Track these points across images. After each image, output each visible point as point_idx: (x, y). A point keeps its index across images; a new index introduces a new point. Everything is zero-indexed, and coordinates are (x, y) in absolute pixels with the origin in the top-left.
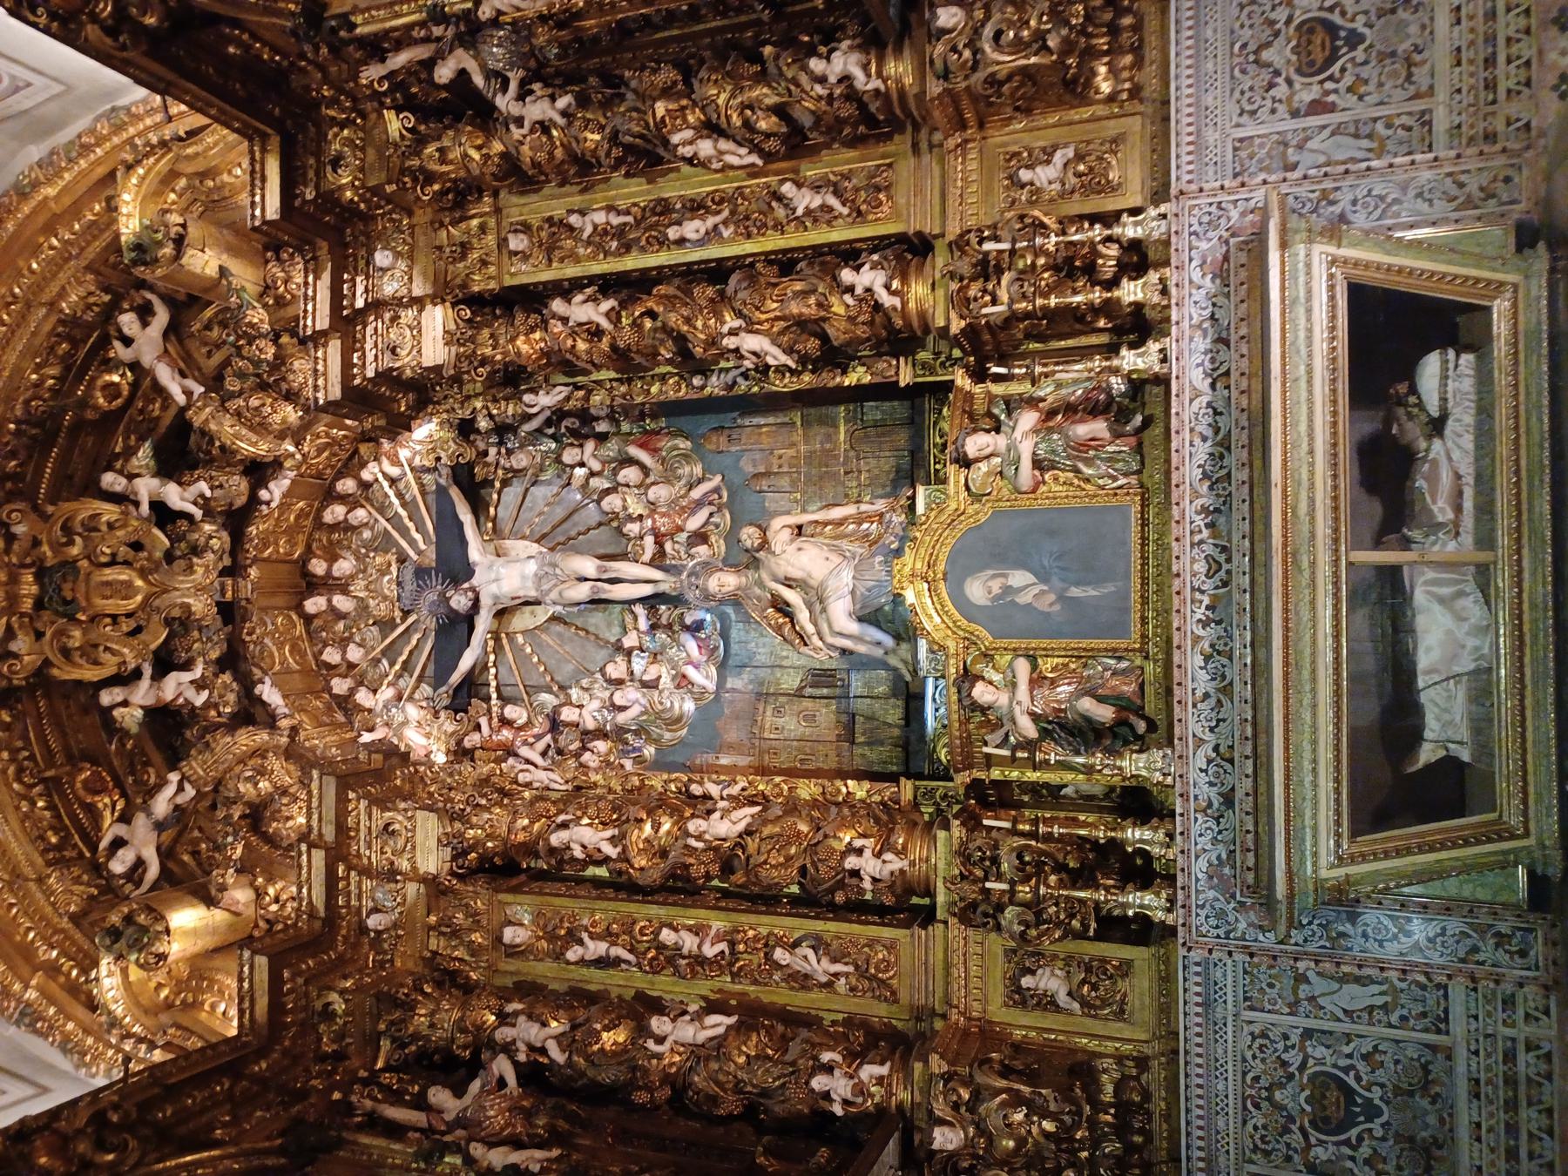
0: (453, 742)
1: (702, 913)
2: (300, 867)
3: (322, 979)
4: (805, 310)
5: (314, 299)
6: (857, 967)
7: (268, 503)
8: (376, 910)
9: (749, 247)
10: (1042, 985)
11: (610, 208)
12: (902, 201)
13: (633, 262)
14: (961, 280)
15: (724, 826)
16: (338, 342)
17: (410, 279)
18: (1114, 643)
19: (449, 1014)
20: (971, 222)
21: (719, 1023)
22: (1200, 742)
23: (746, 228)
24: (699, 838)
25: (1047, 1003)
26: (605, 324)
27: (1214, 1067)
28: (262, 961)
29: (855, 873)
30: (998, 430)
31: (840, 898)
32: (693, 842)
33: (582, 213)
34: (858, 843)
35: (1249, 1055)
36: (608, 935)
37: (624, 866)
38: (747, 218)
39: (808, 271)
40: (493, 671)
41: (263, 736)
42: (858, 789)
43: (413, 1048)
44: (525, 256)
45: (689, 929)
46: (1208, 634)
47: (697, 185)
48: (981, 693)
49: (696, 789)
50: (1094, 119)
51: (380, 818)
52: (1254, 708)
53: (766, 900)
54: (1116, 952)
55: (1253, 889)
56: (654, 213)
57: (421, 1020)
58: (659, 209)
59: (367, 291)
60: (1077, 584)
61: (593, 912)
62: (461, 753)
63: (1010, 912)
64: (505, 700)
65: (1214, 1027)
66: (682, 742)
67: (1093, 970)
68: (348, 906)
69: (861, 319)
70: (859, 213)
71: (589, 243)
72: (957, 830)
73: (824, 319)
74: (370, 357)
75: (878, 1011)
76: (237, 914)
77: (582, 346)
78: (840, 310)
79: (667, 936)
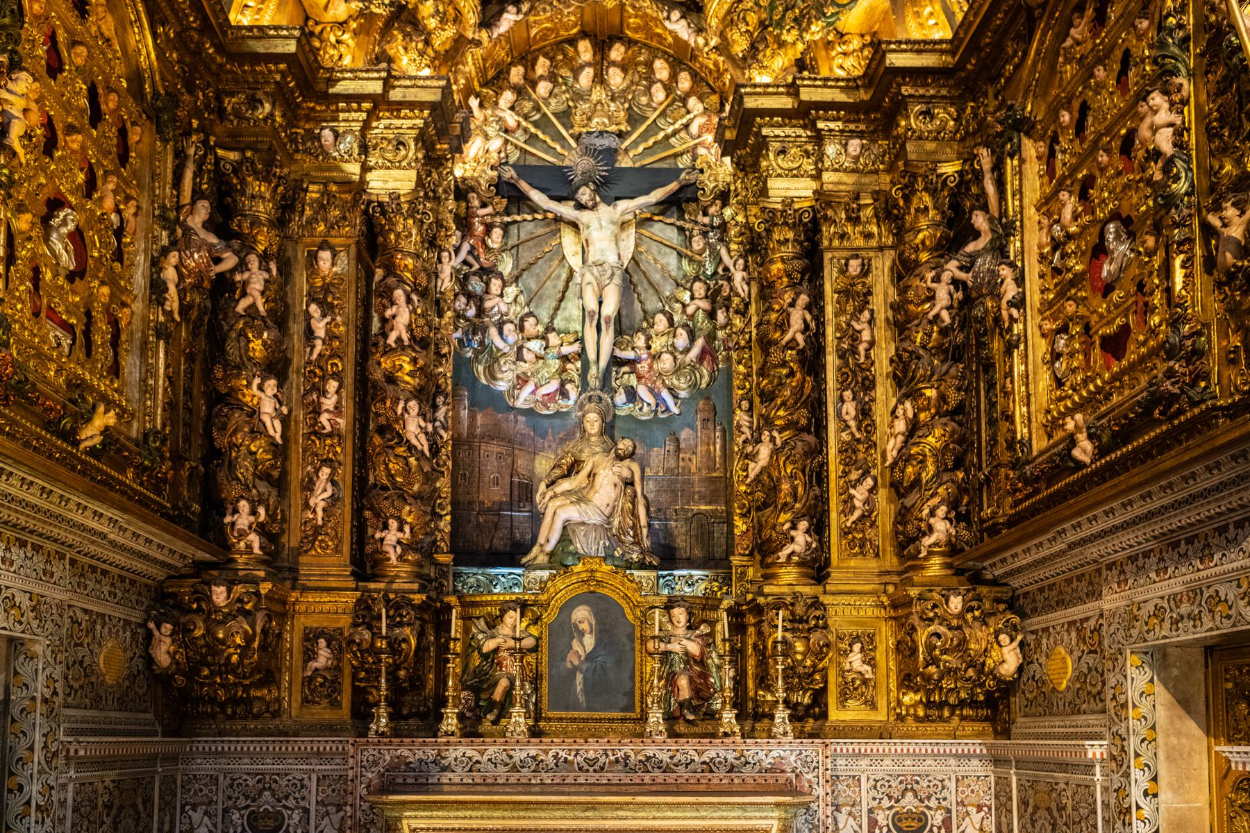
0: (473, 183)
1: (351, 411)
2: (367, 71)
3: (281, 96)
4: (782, 495)
5: (825, 86)
6: (322, 527)
7: (668, 18)
8: (337, 135)
9: (832, 451)
10: (321, 652)
11: (872, 343)
12: (852, 563)
13: (831, 361)
14: (792, 604)
15: (414, 428)
16: (790, 106)
17: (836, 170)
18: (545, 700)
19: (263, 209)
20: (831, 611)
21: (275, 429)
22: (482, 753)
23: (846, 451)
24: (405, 409)
25: (310, 655)
26: (788, 337)
27: (280, 758)
28: (292, 47)
29: (386, 527)
30: (689, 628)
31: (367, 514)
32: (401, 405)
33: (870, 322)
34: (407, 529)
35: (290, 777)
36: (331, 336)
37: (381, 349)
38: (854, 452)
39: (812, 494)
40: (529, 217)
41: (472, 18)
42: (445, 524)
43: (235, 181)
44: (843, 271)
45: (339, 402)
46: (549, 759)
47: (880, 413)
48: (512, 617)
49: (440, 400)
50: (888, 691)
51: (410, 136)
52: (503, 784)
53: (363, 460)
54: (346, 699)
55: (392, 782)
56: (864, 379)
57: (257, 187)
58: (867, 383)
59: (831, 130)
60: (585, 679)
61: (344, 324)
62: (462, 191)
63: (367, 635)
64: (506, 227)
65: (305, 757)
66: (476, 380)
67: (333, 685)
68: (338, 110)
69: (774, 534)
70: (846, 534)
71: (849, 325)
72: (418, 598)
73: (776, 507)
74: (778, 131)
75: (292, 540)
76: (326, 8)
77: (774, 316)
78: (781, 520)
79: (332, 385)
